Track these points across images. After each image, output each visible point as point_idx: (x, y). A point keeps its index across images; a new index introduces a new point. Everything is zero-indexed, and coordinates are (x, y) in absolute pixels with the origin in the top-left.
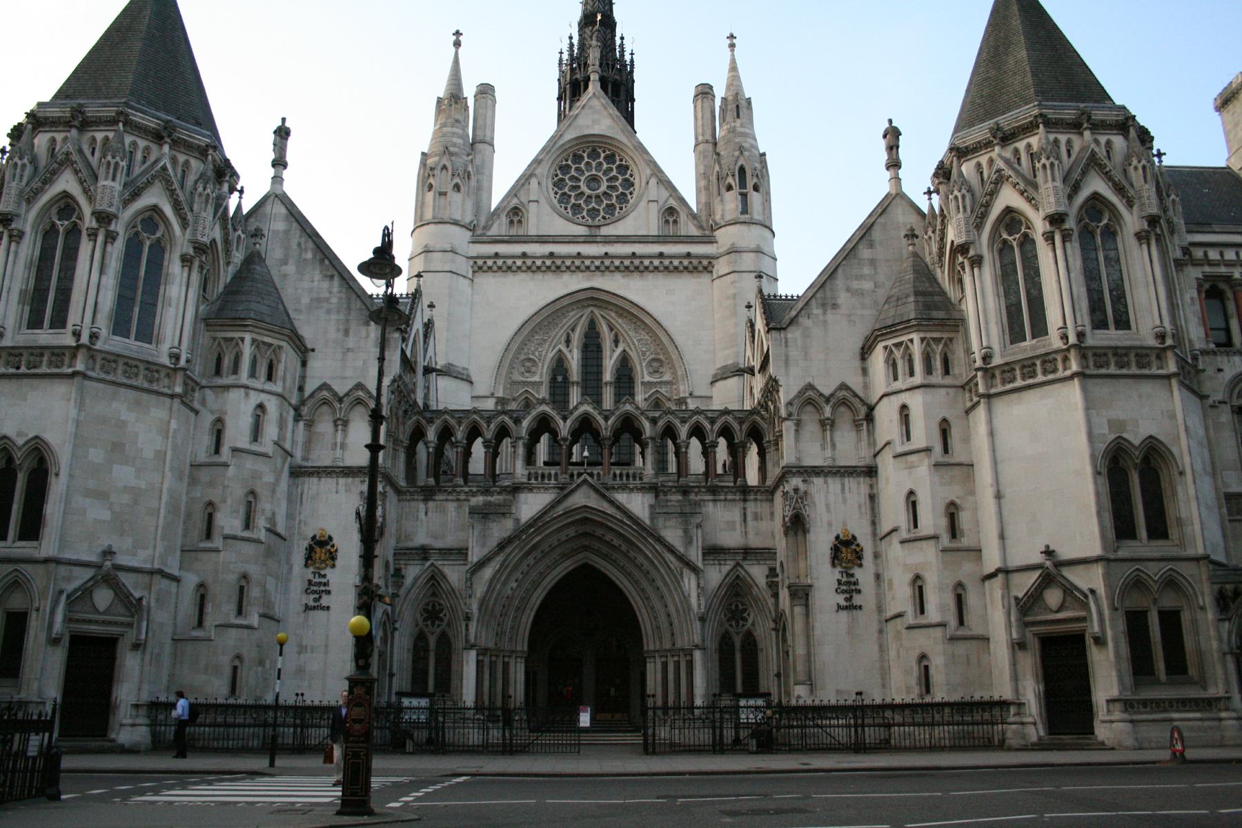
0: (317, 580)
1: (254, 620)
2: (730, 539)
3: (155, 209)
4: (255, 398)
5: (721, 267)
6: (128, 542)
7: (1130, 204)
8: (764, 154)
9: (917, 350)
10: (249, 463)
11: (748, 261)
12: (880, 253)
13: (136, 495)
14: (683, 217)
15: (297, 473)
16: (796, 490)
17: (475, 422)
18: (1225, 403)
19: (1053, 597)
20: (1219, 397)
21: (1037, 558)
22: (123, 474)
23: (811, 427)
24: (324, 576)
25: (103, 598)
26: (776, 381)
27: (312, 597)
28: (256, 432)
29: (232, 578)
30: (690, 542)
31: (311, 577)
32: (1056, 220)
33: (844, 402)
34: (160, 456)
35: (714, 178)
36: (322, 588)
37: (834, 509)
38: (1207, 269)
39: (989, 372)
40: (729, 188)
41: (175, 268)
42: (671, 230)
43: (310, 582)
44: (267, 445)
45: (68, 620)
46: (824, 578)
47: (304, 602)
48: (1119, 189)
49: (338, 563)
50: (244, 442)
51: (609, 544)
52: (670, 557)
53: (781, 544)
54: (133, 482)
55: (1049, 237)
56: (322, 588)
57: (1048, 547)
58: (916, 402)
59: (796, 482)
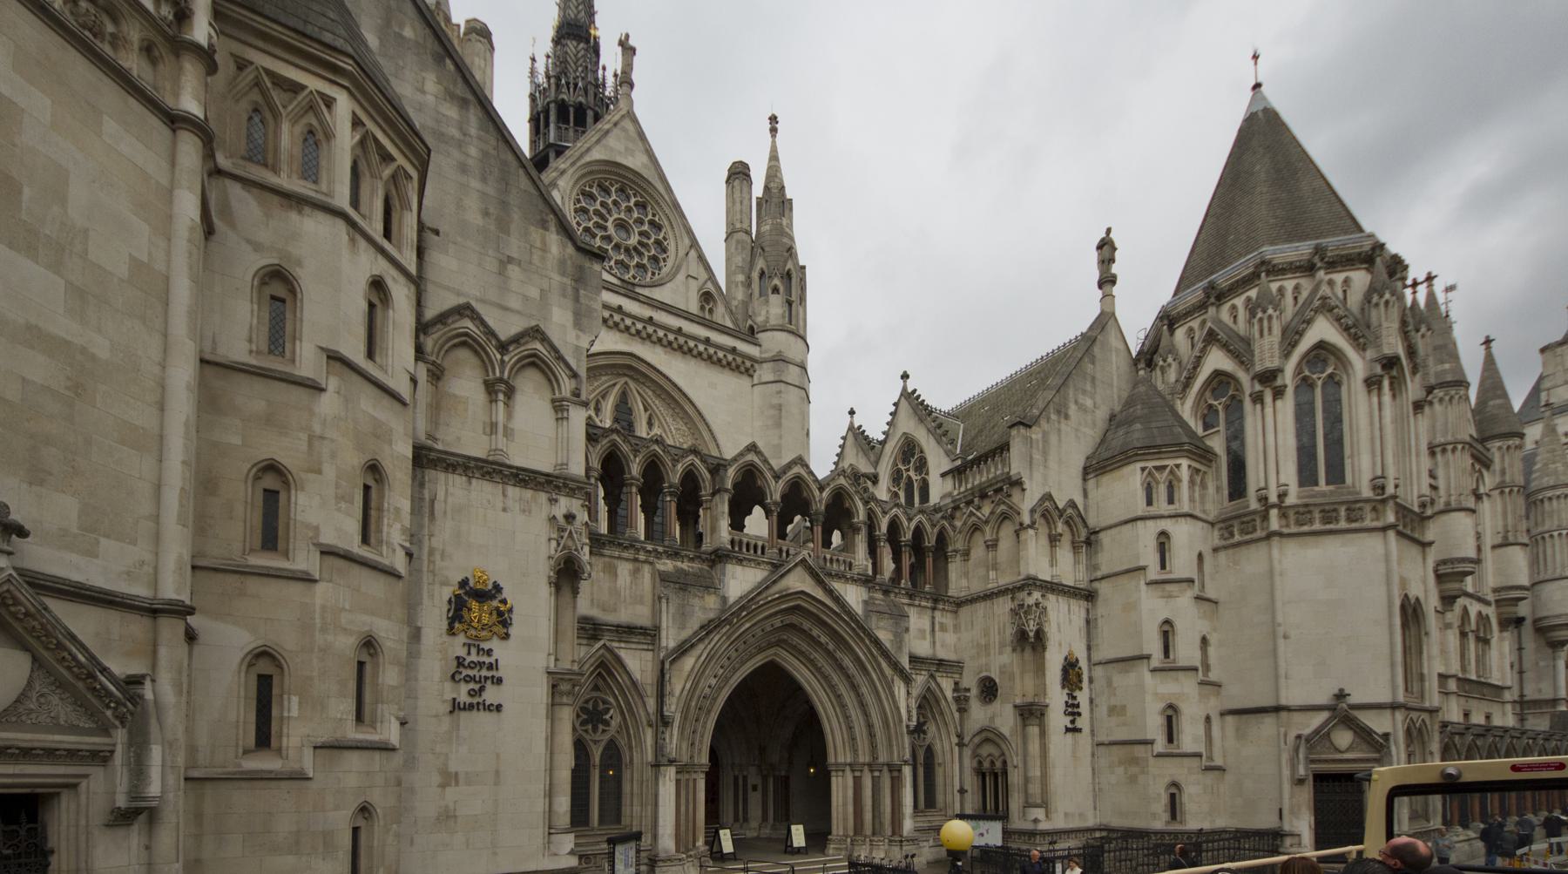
0: (474, 657)
8: (803, 267)
16: (1037, 605)
17: (655, 455)
21: (1323, 698)
24: (489, 652)
27: (464, 688)
30: (900, 648)
31: (462, 652)
35: (755, 275)
36: (484, 673)
40: (776, 290)
43: (460, 662)
47: (449, 696)
49: (513, 631)
51: (815, 642)
52: (884, 665)
56: (484, 673)
57: (1341, 690)
59: (1037, 595)
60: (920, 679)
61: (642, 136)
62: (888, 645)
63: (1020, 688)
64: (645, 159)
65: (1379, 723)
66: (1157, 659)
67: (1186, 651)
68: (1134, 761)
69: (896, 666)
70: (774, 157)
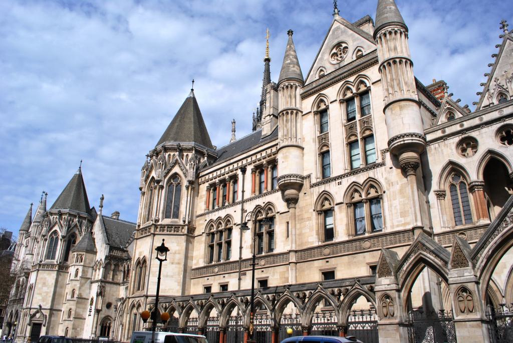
1: (72, 319)
3: (56, 230)
4: (76, 267)
6: (45, 303)
10: (74, 283)
13: (47, 293)
15: (92, 283)
18: (204, 233)
20: (204, 231)
22: (45, 289)
25: (38, 315)
28: (76, 275)
29: (68, 309)
34: (52, 284)
38: (210, 182)
41: (59, 242)
44: (78, 278)
45: (31, 320)
50: (73, 278)
54: (47, 291)
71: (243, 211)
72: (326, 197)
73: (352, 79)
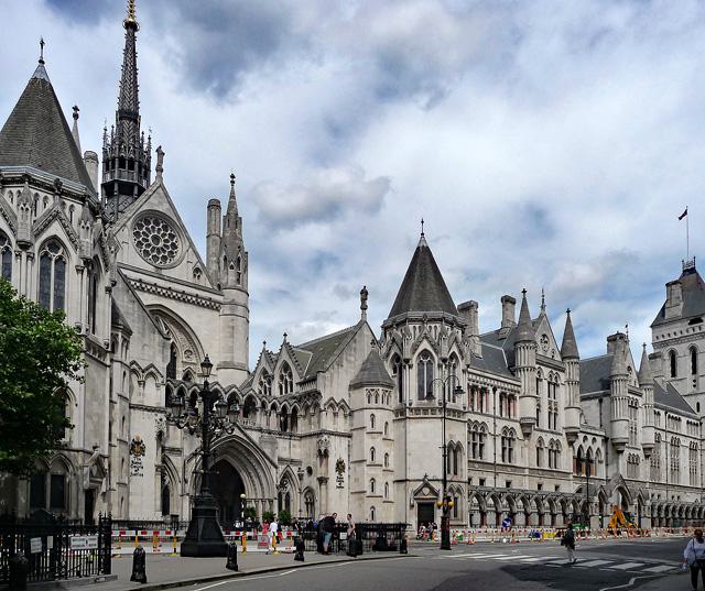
2: (285, 455)
5: (225, 309)
7: (463, 358)
9: (381, 393)
11: (240, 311)
12: (358, 346)
14: (203, 276)
19: (426, 490)
21: (422, 478)
23: (330, 415)
26: (319, 393)
32: (444, 360)
33: (342, 407)
35: (222, 259)
37: (338, 449)
39: (411, 410)
40: (232, 267)
42: (196, 281)
46: (333, 475)
48: (461, 352)
51: (240, 452)
53: (314, 461)
55: (440, 366)
58: (378, 414)
59: (326, 436)
60: (282, 468)
61: (167, 196)
62: (269, 455)
63: (320, 472)
64: (168, 206)
65: (438, 486)
66: (369, 461)
67: (379, 459)
68: (361, 499)
69: (271, 462)
70: (232, 196)
71: (495, 426)
72: (540, 440)
73: (554, 372)
